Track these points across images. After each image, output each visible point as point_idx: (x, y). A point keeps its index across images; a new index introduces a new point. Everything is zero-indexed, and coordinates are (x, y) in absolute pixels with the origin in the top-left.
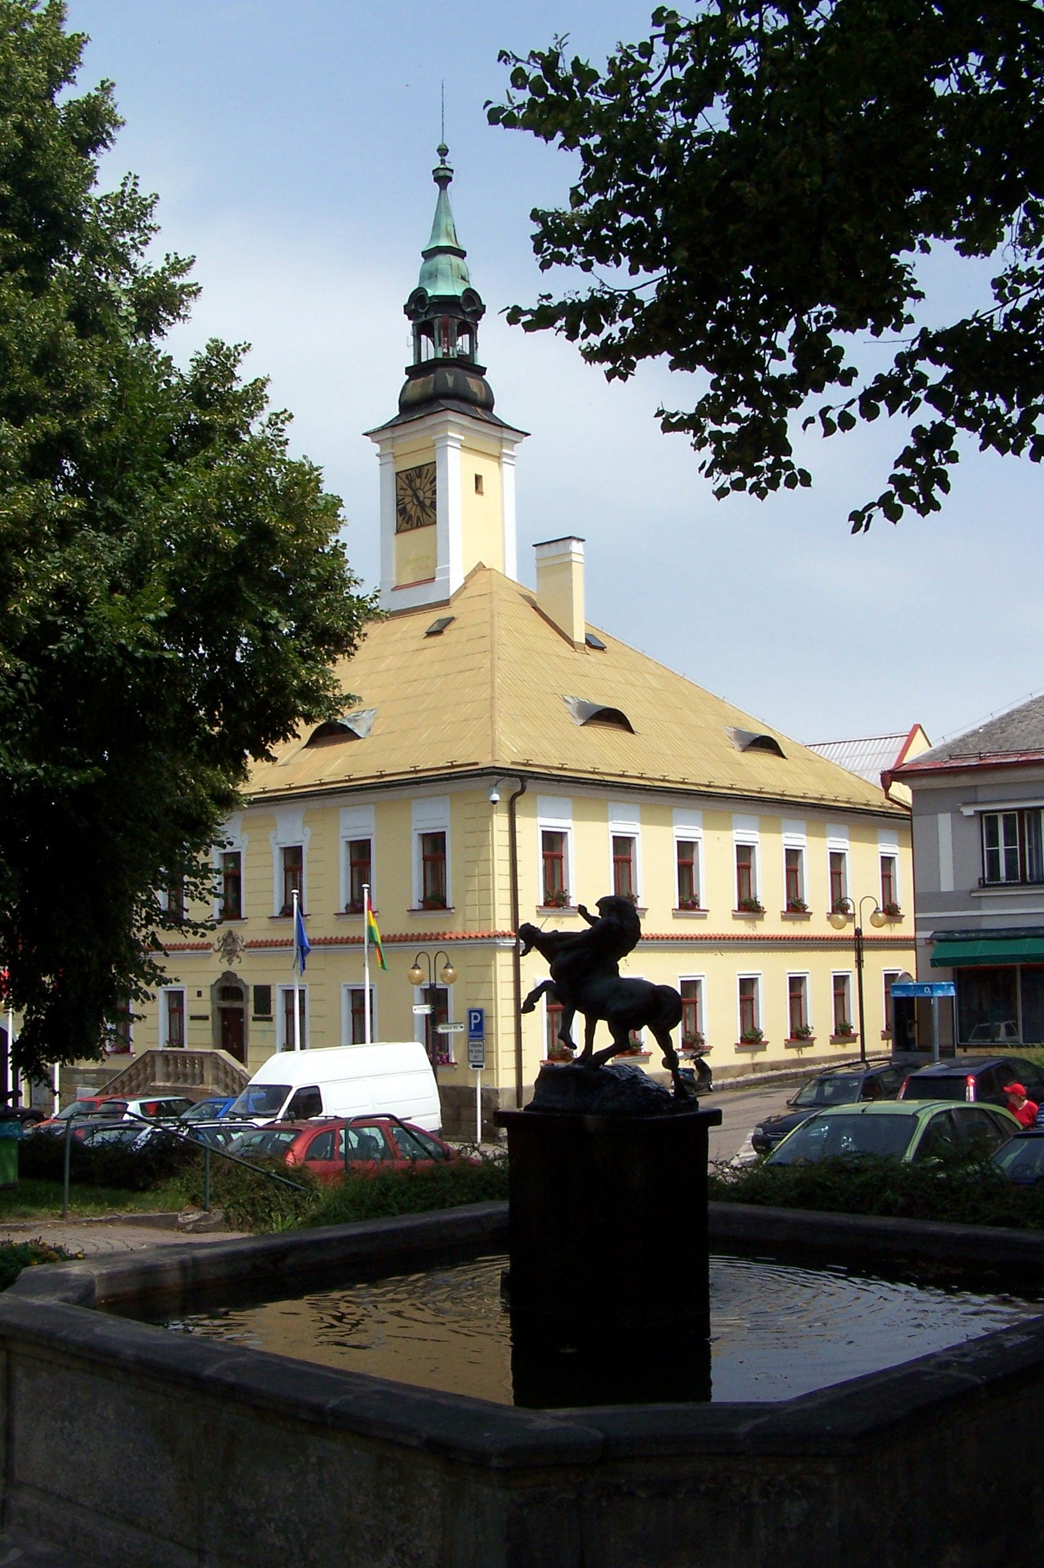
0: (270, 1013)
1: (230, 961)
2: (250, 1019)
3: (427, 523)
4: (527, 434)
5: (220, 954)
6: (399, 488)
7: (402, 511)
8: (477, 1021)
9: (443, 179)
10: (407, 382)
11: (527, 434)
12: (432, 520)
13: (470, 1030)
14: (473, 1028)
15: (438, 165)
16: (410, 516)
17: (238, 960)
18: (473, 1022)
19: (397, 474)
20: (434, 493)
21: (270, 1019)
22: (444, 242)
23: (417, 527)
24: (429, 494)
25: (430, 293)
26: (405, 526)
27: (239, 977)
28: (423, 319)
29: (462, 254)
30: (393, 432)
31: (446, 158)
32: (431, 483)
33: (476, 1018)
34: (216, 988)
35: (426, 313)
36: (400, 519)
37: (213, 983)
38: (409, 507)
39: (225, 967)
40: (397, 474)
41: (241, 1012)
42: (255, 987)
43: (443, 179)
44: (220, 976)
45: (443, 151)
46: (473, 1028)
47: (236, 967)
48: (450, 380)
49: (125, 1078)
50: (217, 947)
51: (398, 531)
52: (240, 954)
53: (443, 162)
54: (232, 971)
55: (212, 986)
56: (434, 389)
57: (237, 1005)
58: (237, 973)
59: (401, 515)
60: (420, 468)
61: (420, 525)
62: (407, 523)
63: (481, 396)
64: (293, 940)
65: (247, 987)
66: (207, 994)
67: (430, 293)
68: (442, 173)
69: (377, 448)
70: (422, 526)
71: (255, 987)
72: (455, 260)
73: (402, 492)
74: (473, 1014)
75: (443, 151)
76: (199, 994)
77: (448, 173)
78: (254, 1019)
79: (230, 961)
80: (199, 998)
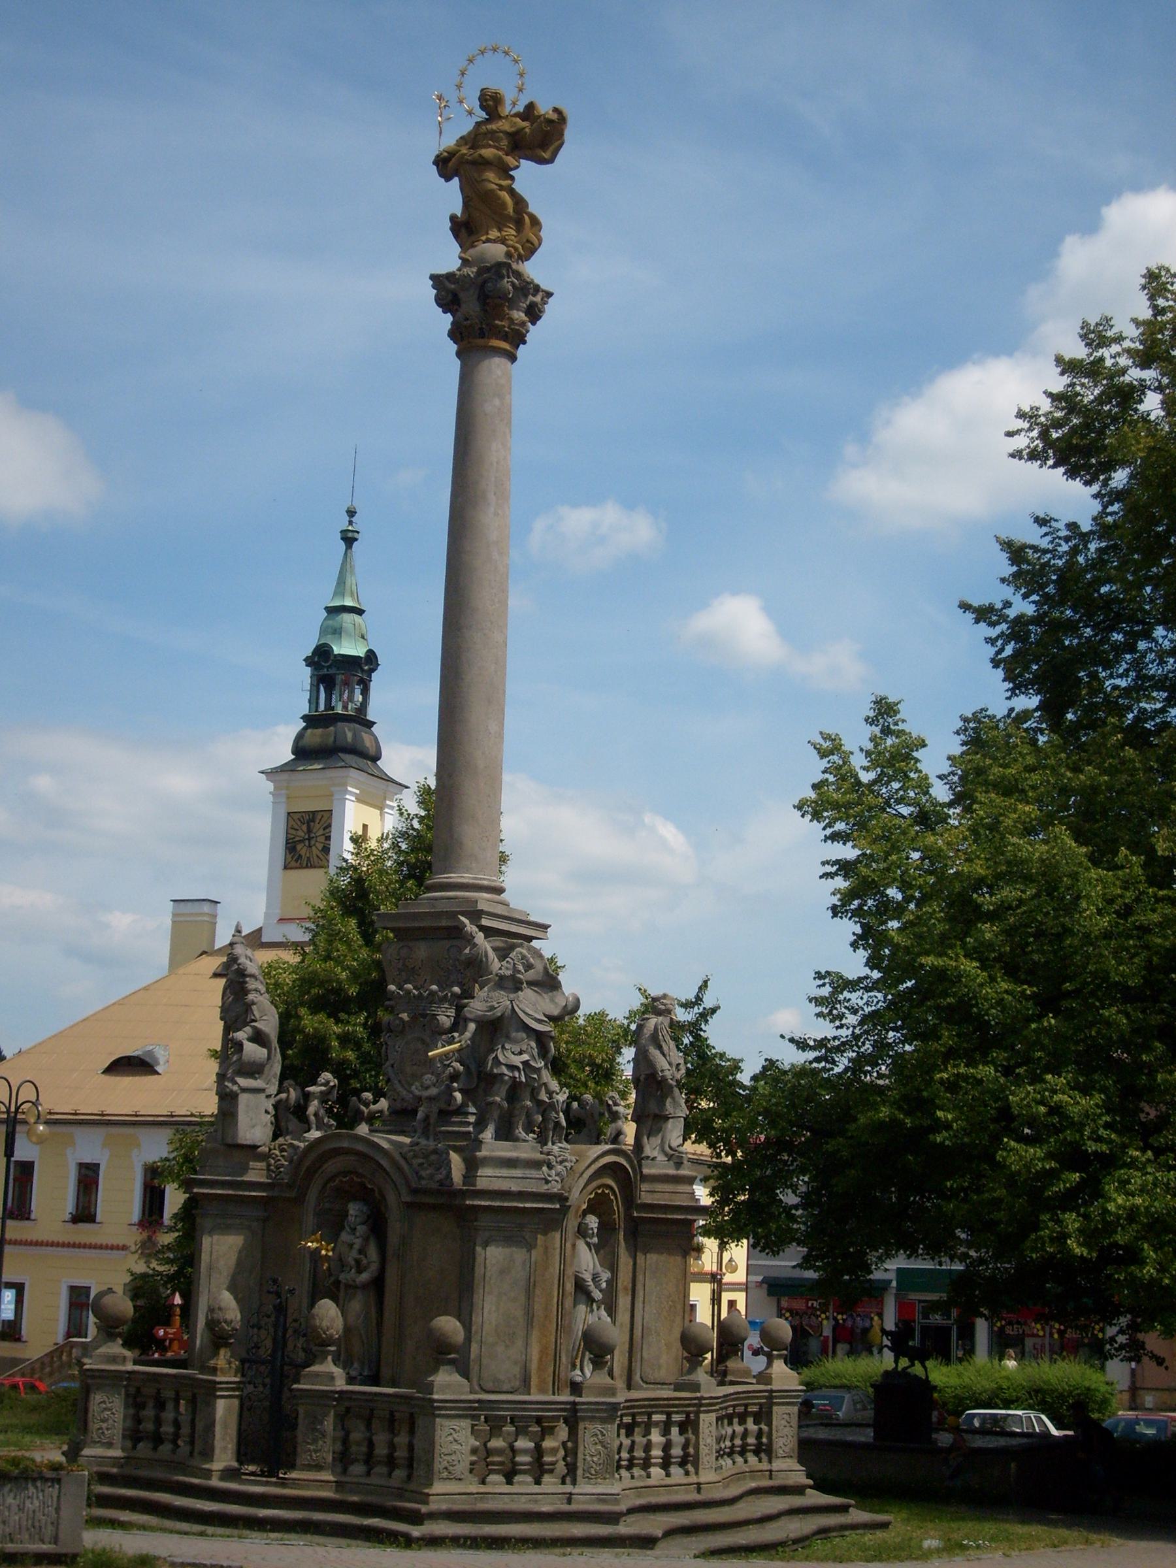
3: (316, 864)
4: (407, 787)
5: (137, 1256)
6: (290, 828)
7: (291, 847)
9: (349, 539)
10: (305, 729)
11: (407, 787)
12: (324, 863)
16: (300, 856)
19: (289, 813)
20: (328, 838)
22: (349, 602)
23: (307, 867)
24: (322, 839)
25: (336, 651)
26: (293, 864)
28: (325, 671)
29: (359, 612)
31: (353, 519)
34: (128, 1288)
35: (328, 667)
36: (289, 857)
40: (289, 813)
43: (349, 539)
45: (351, 513)
48: (349, 735)
49: (37, 1366)
50: (133, 1248)
51: (286, 868)
53: (351, 523)
55: (125, 1285)
56: (335, 741)
60: (314, 812)
62: (296, 861)
63: (372, 751)
67: (336, 651)
68: (350, 535)
69: (270, 786)
70: (312, 867)
72: (356, 617)
73: (293, 832)
75: (351, 513)
77: (356, 535)
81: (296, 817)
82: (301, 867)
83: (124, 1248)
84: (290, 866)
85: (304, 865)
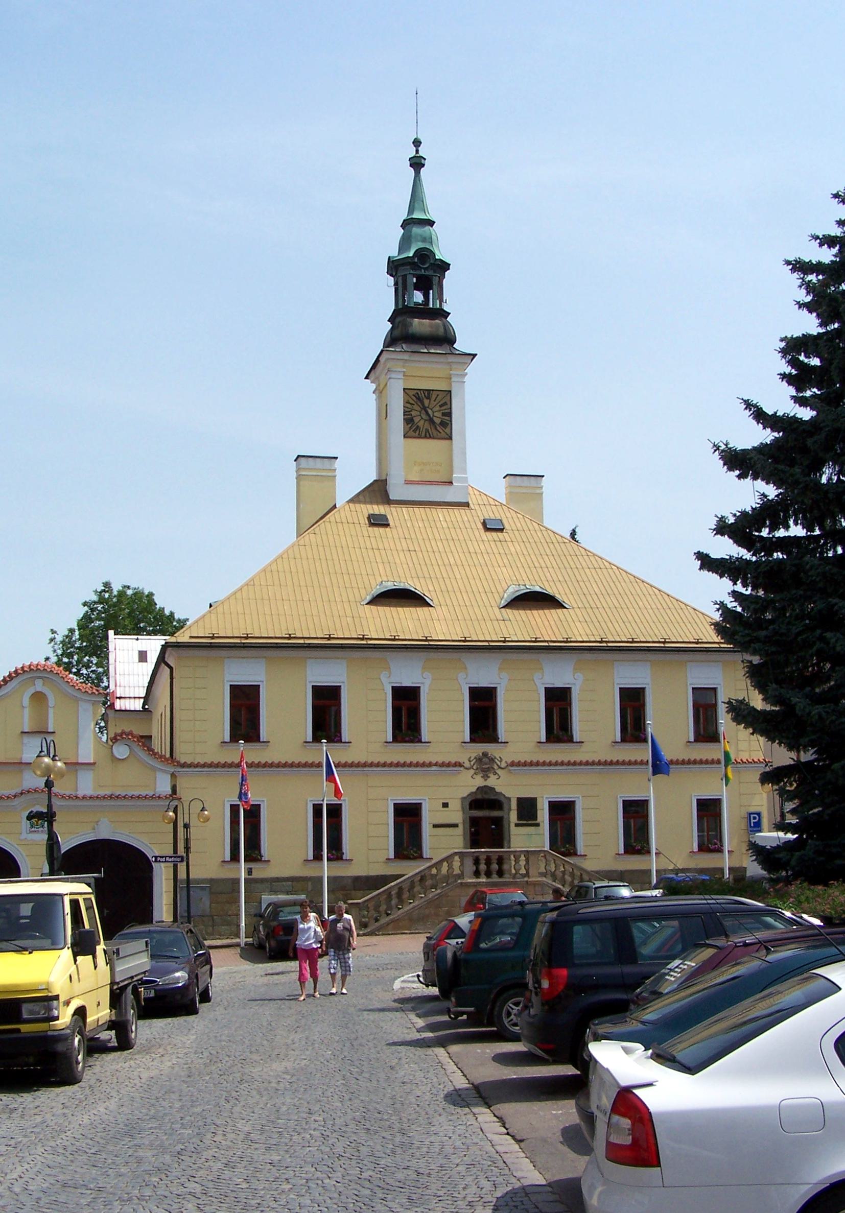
0: (536, 819)
1: (486, 777)
2: (512, 825)
5: (472, 771)
6: (406, 402)
8: (754, 821)
9: (417, 164)
13: (751, 827)
14: (752, 825)
15: (413, 154)
17: (497, 776)
18: (753, 821)
21: (538, 825)
23: (425, 437)
26: (411, 433)
27: (498, 789)
30: (410, 357)
32: (441, 406)
33: (755, 818)
35: (425, 269)
37: (465, 795)
38: (416, 420)
39: (479, 782)
41: (499, 822)
42: (520, 800)
43: (417, 164)
44: (474, 790)
45: (417, 143)
46: (752, 825)
47: (492, 781)
52: (499, 771)
53: (417, 151)
54: (489, 785)
55: (463, 799)
57: (496, 813)
58: (495, 787)
59: (408, 424)
61: (428, 436)
62: (415, 431)
64: (647, 761)
65: (509, 799)
66: (456, 805)
70: (430, 437)
71: (520, 800)
74: (752, 816)
75: (417, 143)
76: (445, 805)
78: (517, 825)
79: (486, 777)
80: (446, 809)
81: (411, 393)
82: (420, 437)
83: (458, 764)
84: (408, 434)
85: (423, 435)
